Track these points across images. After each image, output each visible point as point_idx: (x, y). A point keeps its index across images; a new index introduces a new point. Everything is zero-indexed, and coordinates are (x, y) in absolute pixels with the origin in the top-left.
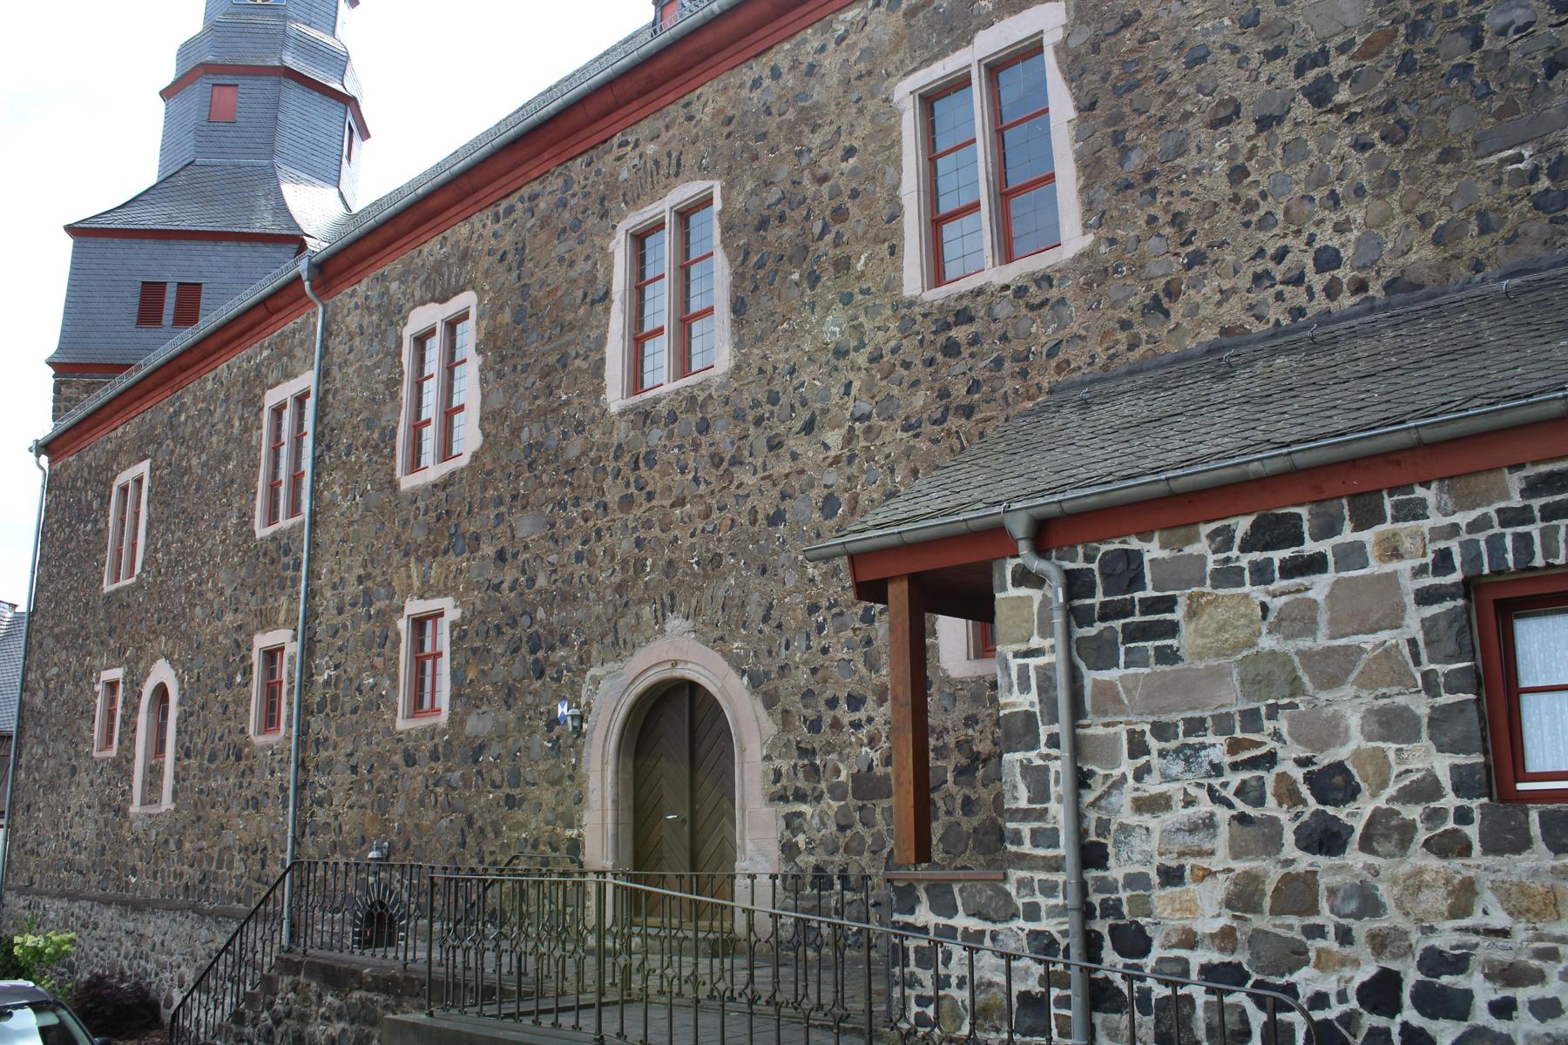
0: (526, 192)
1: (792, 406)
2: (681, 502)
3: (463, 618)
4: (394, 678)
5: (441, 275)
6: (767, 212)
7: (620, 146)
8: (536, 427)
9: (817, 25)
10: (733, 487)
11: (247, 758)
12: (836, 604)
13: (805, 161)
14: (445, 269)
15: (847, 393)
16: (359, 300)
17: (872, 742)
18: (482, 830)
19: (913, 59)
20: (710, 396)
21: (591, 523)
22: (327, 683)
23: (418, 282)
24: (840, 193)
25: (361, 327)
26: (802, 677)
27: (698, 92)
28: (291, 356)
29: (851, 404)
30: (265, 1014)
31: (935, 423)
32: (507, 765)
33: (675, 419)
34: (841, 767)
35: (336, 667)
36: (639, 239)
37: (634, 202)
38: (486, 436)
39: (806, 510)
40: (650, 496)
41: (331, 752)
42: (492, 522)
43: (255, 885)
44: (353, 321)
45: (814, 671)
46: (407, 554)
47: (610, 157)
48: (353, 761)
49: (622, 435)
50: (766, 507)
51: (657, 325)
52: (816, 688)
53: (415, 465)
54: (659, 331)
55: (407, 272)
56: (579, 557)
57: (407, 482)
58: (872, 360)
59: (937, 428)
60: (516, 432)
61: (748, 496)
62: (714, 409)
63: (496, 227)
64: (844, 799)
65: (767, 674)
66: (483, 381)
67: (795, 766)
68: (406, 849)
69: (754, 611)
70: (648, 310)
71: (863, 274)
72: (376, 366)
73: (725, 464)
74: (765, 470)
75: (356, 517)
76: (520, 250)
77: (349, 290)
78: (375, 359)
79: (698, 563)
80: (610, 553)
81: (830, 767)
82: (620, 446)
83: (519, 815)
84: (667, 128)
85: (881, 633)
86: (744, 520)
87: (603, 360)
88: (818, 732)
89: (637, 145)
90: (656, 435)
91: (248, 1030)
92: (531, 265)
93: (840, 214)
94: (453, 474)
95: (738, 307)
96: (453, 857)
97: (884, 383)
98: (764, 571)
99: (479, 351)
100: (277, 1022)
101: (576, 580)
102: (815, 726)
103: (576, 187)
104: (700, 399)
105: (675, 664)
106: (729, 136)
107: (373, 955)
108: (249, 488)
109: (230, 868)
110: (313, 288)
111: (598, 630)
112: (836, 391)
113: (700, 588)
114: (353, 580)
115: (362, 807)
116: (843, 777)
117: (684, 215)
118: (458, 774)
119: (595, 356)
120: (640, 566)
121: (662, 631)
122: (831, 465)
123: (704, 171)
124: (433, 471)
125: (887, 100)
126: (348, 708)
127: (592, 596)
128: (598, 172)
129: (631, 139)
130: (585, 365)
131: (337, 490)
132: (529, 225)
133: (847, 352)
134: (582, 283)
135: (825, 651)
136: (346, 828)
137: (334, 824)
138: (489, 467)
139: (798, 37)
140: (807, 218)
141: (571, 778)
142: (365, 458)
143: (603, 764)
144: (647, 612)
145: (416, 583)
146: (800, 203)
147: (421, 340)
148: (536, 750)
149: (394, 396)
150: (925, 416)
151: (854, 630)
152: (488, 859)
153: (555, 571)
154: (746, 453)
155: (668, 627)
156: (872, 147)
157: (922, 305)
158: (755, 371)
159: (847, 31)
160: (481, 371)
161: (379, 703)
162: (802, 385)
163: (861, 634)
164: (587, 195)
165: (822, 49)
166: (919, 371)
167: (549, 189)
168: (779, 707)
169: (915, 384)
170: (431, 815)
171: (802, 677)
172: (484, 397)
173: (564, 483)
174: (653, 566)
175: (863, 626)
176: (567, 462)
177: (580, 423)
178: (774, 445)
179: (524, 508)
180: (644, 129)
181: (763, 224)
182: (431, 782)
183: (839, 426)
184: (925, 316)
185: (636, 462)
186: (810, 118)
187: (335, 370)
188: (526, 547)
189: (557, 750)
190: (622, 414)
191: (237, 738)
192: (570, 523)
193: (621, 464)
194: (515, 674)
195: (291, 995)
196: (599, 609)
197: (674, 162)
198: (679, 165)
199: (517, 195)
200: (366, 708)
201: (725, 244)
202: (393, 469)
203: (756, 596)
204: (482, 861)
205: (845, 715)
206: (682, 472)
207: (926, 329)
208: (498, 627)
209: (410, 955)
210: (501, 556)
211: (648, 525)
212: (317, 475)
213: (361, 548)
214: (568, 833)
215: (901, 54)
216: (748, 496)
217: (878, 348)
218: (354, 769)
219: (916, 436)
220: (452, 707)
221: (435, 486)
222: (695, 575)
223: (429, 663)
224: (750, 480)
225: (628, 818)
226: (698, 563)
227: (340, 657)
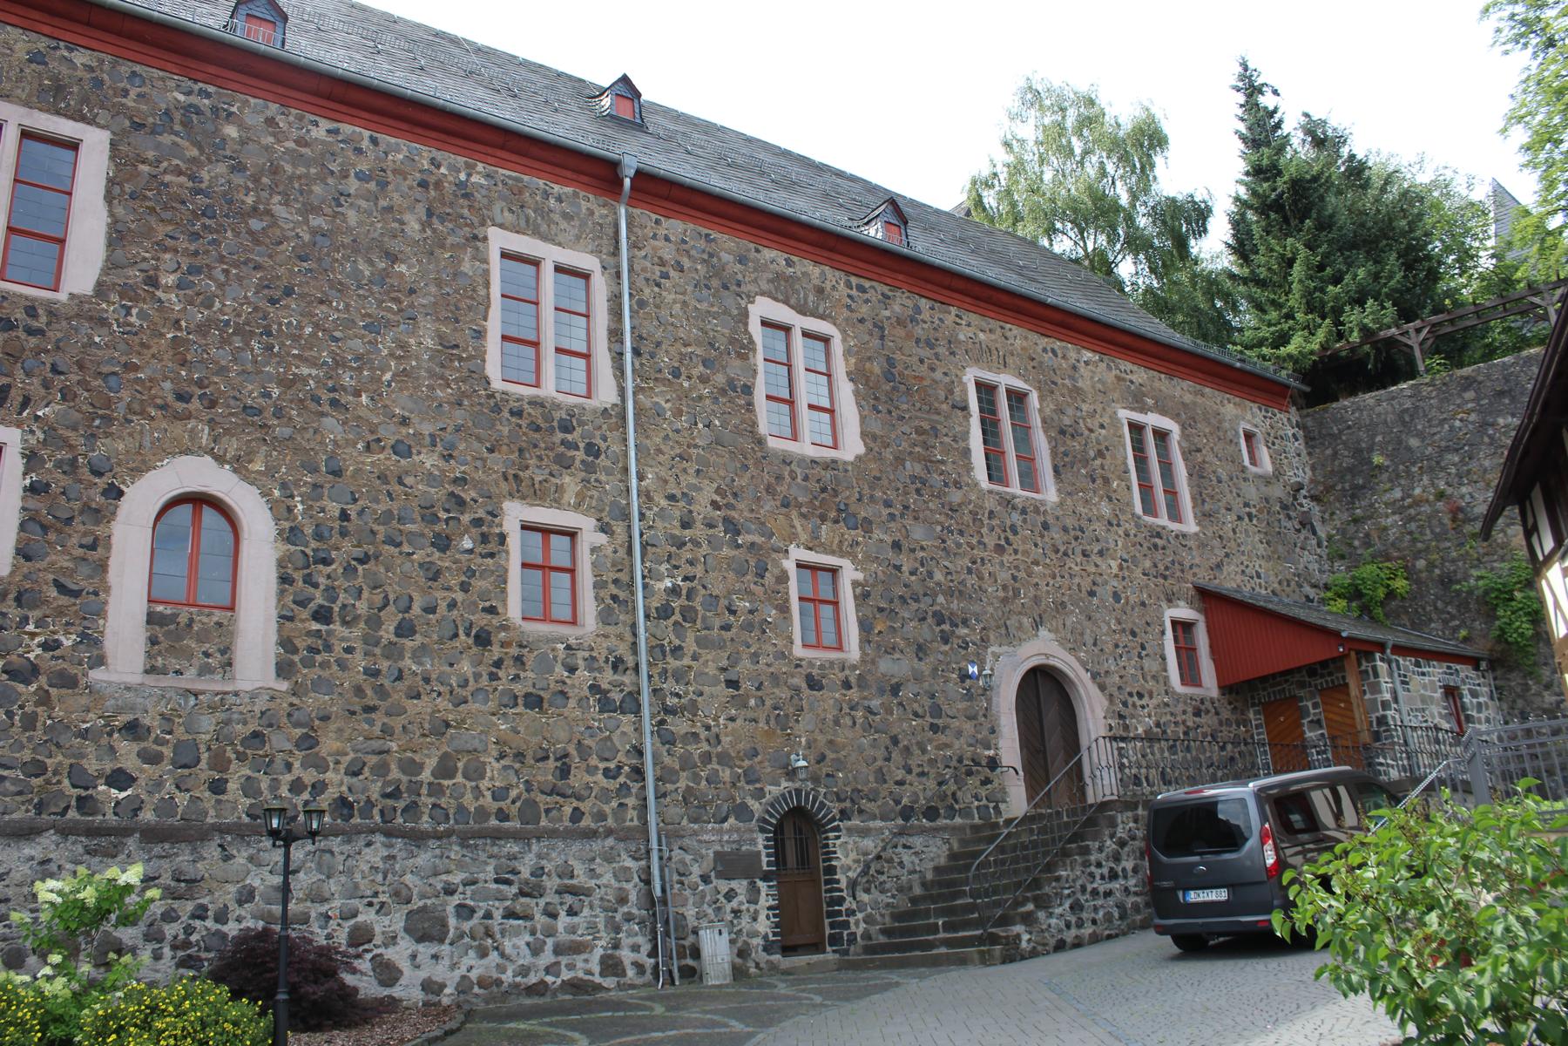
18: (907, 749)
40: (1016, 552)
43: (540, 798)
62: (1051, 521)
69: (1089, 640)
83: (942, 738)
102: (1125, 704)
120: (1016, 593)
144: (1026, 621)
196: (991, 609)
218: (733, 684)
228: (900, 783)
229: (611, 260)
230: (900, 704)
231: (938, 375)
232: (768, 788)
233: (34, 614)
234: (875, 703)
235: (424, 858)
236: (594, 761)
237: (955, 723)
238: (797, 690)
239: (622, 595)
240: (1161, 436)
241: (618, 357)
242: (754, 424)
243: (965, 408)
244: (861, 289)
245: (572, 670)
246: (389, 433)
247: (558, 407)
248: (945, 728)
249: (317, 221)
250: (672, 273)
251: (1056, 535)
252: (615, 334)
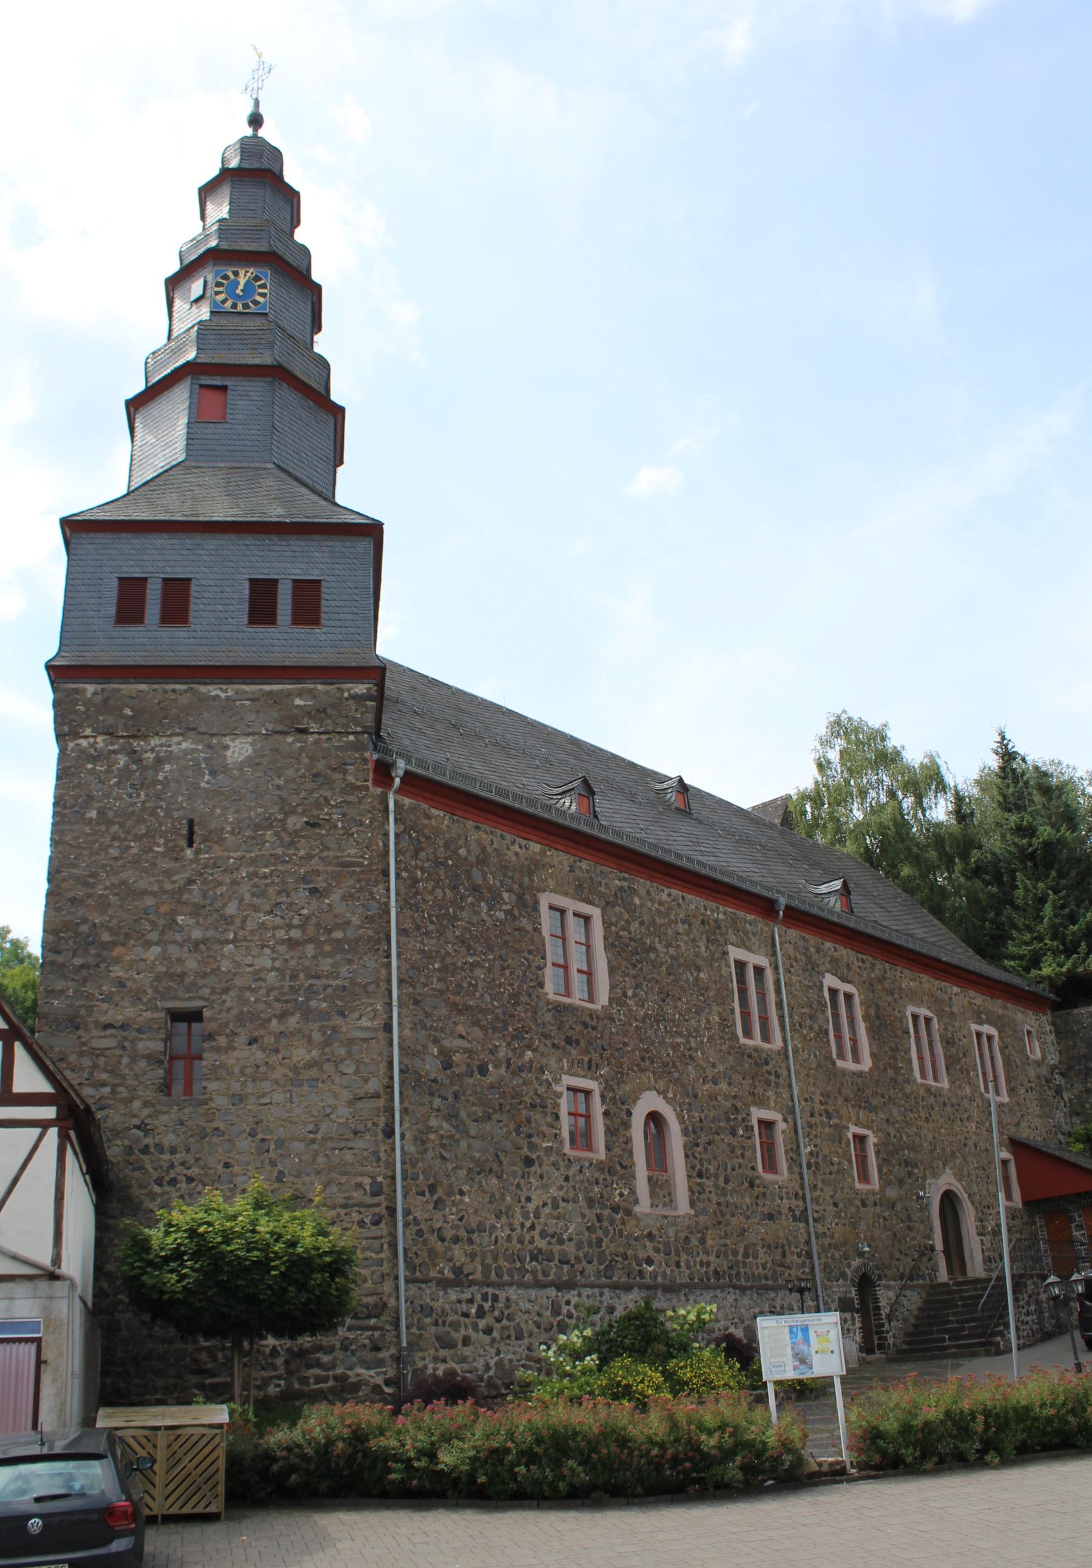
4: (850, 1162)
11: (758, 1187)
43: (778, 1268)
83: (913, 1234)
108: (792, 1025)
109: (755, 1257)
136: (836, 1235)
144: (940, 1164)
191: (750, 1173)
218: (835, 1205)
228: (898, 1260)
229: (773, 959)
231: (896, 1013)
232: (852, 1262)
233: (615, 1178)
234: (886, 1214)
235: (746, 1301)
236: (793, 1249)
237: (916, 1225)
238: (858, 1207)
239: (795, 1157)
240: (990, 1038)
241: (781, 1018)
242: (831, 1053)
243: (908, 1033)
244: (863, 961)
245: (782, 1199)
246: (709, 1072)
247: (762, 1050)
249: (672, 951)
250: (794, 964)
251: (949, 1109)
252: (779, 1005)
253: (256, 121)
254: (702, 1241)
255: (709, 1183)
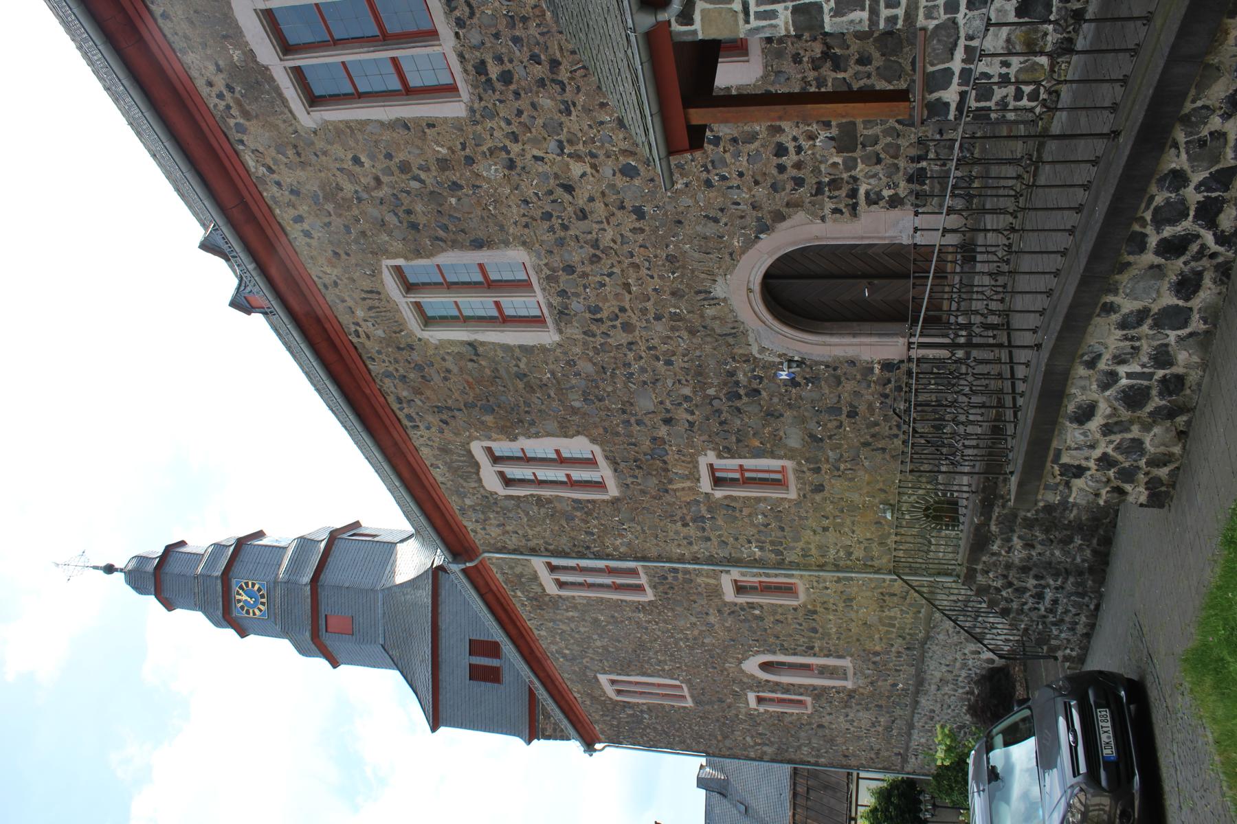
0: (395, 406)
1: (553, 202)
2: (627, 286)
3: (714, 449)
4: (758, 500)
5: (459, 468)
6: (405, 224)
7: (358, 336)
8: (571, 396)
9: (261, 189)
10: (615, 247)
11: (815, 606)
12: (705, 166)
13: (365, 196)
14: (455, 465)
15: (542, 159)
16: (479, 527)
17: (812, 137)
18: (873, 436)
19: (282, 113)
20: (546, 265)
21: (643, 354)
22: (761, 549)
23: (465, 484)
24: (388, 167)
25: (499, 526)
26: (761, 192)
27: (316, 279)
28: (521, 576)
29: (551, 156)
30: (1004, 593)
31: (564, 90)
32: (825, 417)
33: (564, 291)
34: (831, 161)
35: (750, 542)
36: (428, 321)
37: (400, 326)
38: (578, 433)
39: (633, 190)
40: (622, 310)
41: (812, 546)
42: (643, 428)
43: (908, 601)
44: (495, 532)
45: (757, 183)
46: (667, 491)
47: (368, 344)
48: (819, 530)
49: (576, 331)
50: (630, 221)
51: (493, 306)
52: (770, 181)
53: (600, 485)
54: (497, 304)
55: (457, 493)
56: (669, 363)
57: (613, 491)
58: (516, 140)
59: (568, 88)
60: (575, 411)
61: (622, 235)
62: (556, 261)
63: (422, 427)
64: (855, 160)
65: (759, 219)
66: (537, 435)
67: (830, 197)
68: (885, 491)
69: (710, 229)
70: (482, 313)
71: (450, 148)
72: (527, 514)
73: (598, 253)
74: (602, 222)
75: (639, 528)
76: (440, 410)
77: (472, 534)
78: (522, 515)
79: (673, 273)
80: (666, 340)
81: (830, 170)
82: (585, 333)
83: (862, 408)
84: (343, 301)
85: (727, 131)
86: (640, 238)
87: (520, 347)
88: (803, 180)
89: (357, 324)
90: (576, 305)
91: (1015, 605)
92: (450, 402)
93: (405, 167)
94: (607, 458)
95: (478, 244)
96: (893, 457)
97: (533, 130)
98: (680, 222)
99: (515, 439)
100: (1010, 584)
101: (686, 365)
102: (799, 182)
103: (391, 369)
104: (549, 273)
105: (750, 290)
106: (348, 254)
107: (964, 515)
108: (619, 605)
110: (471, 560)
111: (724, 349)
112: (540, 167)
113: (693, 271)
114: (685, 530)
115: (853, 523)
116: (839, 160)
117: (409, 288)
118: (830, 453)
119: (517, 352)
120: (675, 317)
121: (725, 300)
122: (598, 171)
123: (375, 273)
124: (604, 472)
125: (315, 133)
126: (780, 534)
127: (698, 353)
128: (379, 352)
129: (353, 328)
130: (524, 360)
131: (618, 542)
132: (419, 403)
133: (511, 160)
134: (462, 363)
135: (741, 175)
136: (868, 535)
137: (866, 544)
138: (601, 431)
139: (270, 203)
140: (408, 193)
141: (835, 369)
142: (595, 522)
143: (825, 344)
144: (710, 312)
145: (688, 484)
146: (398, 199)
147: (508, 482)
148: (815, 395)
149: (549, 501)
150: (559, 98)
151: (725, 151)
152: (895, 431)
153: (679, 381)
154: (589, 237)
155: (722, 295)
156: (352, 143)
157: (472, 101)
158: (527, 231)
159: (263, 165)
160: (529, 437)
161: (776, 511)
162: (536, 194)
163: (728, 147)
164: (396, 361)
165: (278, 184)
166: (523, 103)
167: (393, 389)
168: (784, 210)
169: (534, 105)
170: (861, 473)
171: (761, 192)
172: (549, 435)
173: (613, 375)
174: (675, 307)
175: (722, 144)
176: (597, 372)
177: (568, 363)
178: (583, 215)
179: (632, 404)
180: (345, 319)
181: (414, 226)
182: (836, 473)
183: (568, 165)
184: (481, 99)
185: (597, 320)
186: (332, 193)
187: (531, 544)
188: (661, 403)
189: (814, 380)
190: (560, 332)
191: (800, 614)
192: (643, 370)
193: (598, 332)
194: (756, 410)
195: (991, 575)
197: (369, 296)
198: (371, 292)
199: (398, 412)
200: (780, 521)
201: (430, 255)
202: (603, 501)
203: (699, 228)
204: (896, 436)
205: (790, 160)
206: (604, 285)
207: (491, 98)
208: (721, 423)
209: (965, 489)
210: (668, 421)
211: (644, 311)
212: (608, 557)
213: (662, 524)
214: (877, 371)
215: (279, 122)
216: (622, 235)
217: (507, 136)
218: (825, 529)
219: (574, 104)
220: (780, 458)
221: (616, 470)
222: (683, 275)
223: (747, 475)
224: (610, 233)
225: (867, 326)
226: (673, 273)
227: (742, 539)
230: (830, 437)
237: (845, 396)
248: (851, 405)
253: (110, 569)
254: (876, 654)
255: (817, 644)
